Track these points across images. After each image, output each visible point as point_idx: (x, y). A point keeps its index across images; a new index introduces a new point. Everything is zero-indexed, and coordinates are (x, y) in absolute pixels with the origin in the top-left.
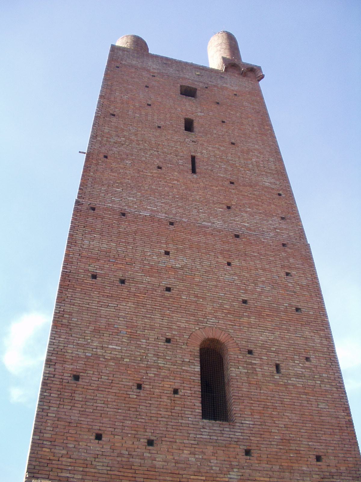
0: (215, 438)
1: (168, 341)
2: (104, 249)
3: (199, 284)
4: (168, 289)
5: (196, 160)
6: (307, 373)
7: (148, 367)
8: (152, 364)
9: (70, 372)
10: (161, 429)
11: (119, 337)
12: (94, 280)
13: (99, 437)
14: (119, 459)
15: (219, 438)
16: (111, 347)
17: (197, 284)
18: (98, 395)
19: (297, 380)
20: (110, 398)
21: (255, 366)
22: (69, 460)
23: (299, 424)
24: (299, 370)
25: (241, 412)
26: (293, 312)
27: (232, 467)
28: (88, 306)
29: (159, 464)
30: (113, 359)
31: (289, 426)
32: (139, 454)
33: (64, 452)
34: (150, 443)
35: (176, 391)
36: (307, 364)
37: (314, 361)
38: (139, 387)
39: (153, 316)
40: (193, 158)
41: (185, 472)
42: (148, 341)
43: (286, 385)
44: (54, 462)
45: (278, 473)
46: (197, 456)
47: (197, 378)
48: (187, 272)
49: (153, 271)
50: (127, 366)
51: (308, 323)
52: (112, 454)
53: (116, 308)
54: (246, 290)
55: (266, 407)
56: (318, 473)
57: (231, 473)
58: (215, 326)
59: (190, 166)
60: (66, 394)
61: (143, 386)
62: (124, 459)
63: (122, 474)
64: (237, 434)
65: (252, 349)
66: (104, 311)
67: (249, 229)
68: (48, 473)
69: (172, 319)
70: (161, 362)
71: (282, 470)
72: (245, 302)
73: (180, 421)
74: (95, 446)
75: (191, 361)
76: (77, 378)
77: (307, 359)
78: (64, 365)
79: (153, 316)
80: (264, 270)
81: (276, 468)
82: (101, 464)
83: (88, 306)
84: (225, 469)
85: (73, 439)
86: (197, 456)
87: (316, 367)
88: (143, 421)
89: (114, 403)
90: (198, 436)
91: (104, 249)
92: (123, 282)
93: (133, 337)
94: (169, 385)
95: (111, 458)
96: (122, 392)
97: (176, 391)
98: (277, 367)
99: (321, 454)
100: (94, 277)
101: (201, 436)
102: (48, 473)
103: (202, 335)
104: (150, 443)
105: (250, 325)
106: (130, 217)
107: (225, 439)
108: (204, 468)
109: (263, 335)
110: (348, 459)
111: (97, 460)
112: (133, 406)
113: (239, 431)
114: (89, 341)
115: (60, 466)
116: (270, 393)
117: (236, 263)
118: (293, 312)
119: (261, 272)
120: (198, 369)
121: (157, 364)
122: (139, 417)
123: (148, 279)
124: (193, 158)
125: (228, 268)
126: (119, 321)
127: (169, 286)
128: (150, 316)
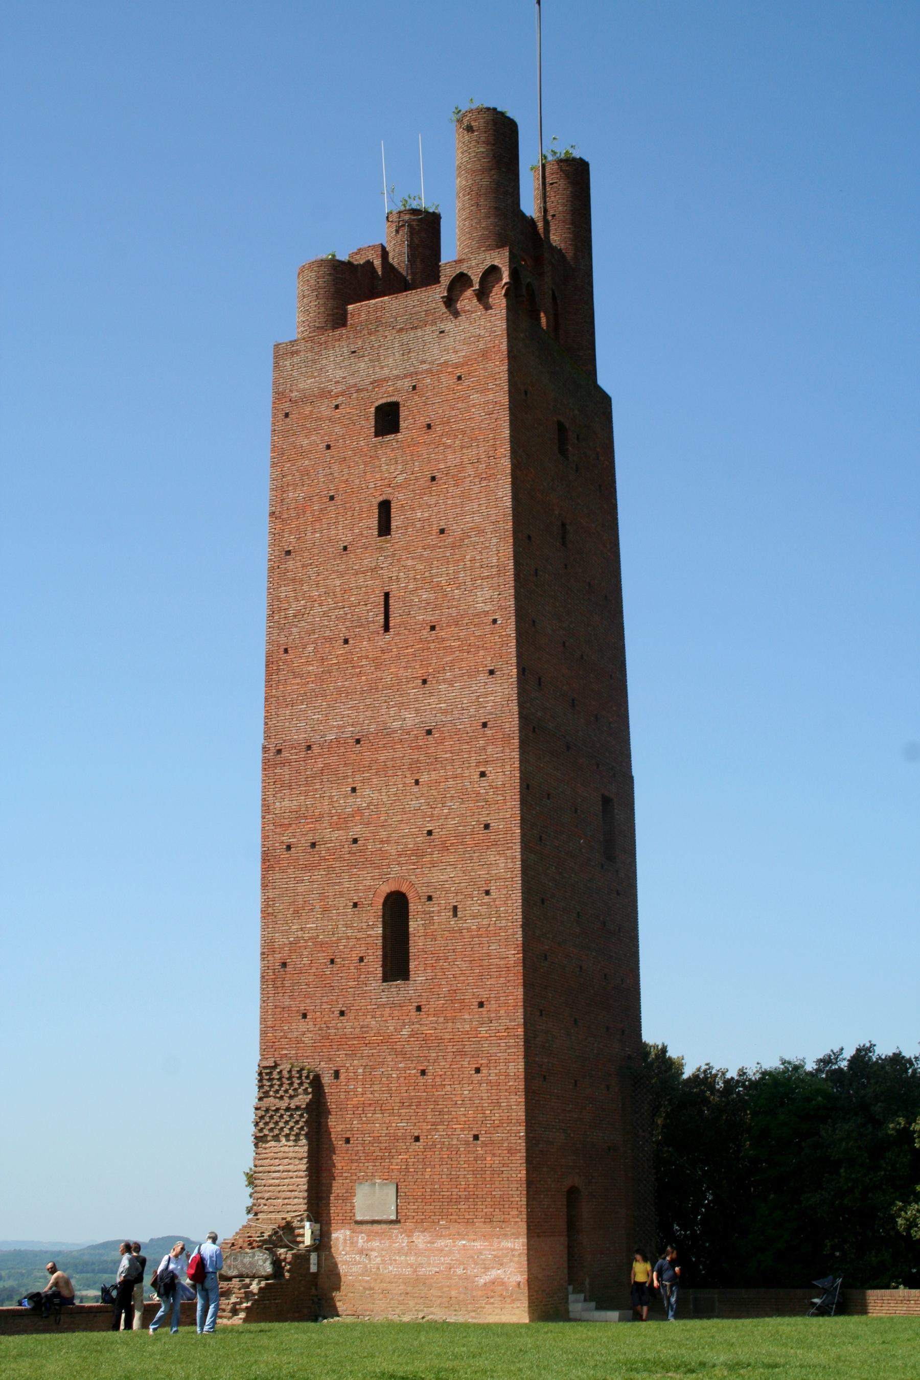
0: (392, 999)
1: (355, 905)
2: (294, 807)
3: (385, 824)
4: (355, 841)
5: (391, 601)
6: (484, 910)
7: (339, 939)
8: (342, 935)
9: (279, 961)
10: (350, 999)
11: (314, 913)
12: (289, 852)
13: (305, 1016)
14: (320, 1032)
15: (396, 999)
16: (308, 926)
17: (382, 824)
18: (302, 978)
19: (472, 921)
20: (311, 978)
21: (432, 915)
22: (286, 1040)
23: (467, 972)
24: (476, 908)
25: (416, 969)
26: (480, 832)
27: (404, 1025)
28: (286, 886)
29: (348, 1031)
30: (310, 938)
31: (458, 976)
32: (334, 1025)
33: (282, 1034)
34: (342, 1013)
35: (361, 959)
36: (486, 899)
37: (494, 894)
38: (332, 961)
39: (341, 881)
40: (387, 595)
41: (368, 1035)
42: (338, 911)
43: (460, 931)
44: (276, 1044)
45: (442, 1025)
46: (377, 1019)
47: (380, 942)
48: (374, 810)
49: (342, 822)
50: (322, 944)
51: (495, 844)
52: (315, 1029)
53: (310, 880)
54: (432, 815)
55: (438, 960)
56: (478, 1019)
57: (403, 1030)
58: (398, 875)
59: (381, 618)
60: (279, 983)
61: (336, 960)
62: (323, 1032)
63: (322, 1044)
64: (410, 992)
65: (431, 894)
66: (301, 888)
67: (445, 712)
68: (273, 1053)
69: (358, 879)
70: (349, 932)
71: (446, 1020)
72: (430, 833)
73: (365, 988)
74: (303, 1026)
75: (375, 923)
76: (284, 965)
77: (487, 893)
78: (275, 955)
79: (341, 881)
80: (455, 777)
81: (441, 1020)
82: (307, 1039)
83: (286, 886)
84: (399, 1027)
85: (287, 1022)
86: (377, 1019)
87: (494, 900)
88: (336, 994)
89: (314, 983)
90: (379, 1000)
91: (294, 807)
92: (313, 845)
93: (325, 910)
94: (355, 956)
95: (314, 1032)
96: (319, 970)
97: (361, 959)
98: (455, 908)
99: (483, 1000)
100: (289, 848)
101: (381, 1000)
102: (273, 1053)
103: (386, 889)
104: (342, 1013)
105: (433, 864)
106: (316, 749)
107: (400, 999)
108: (382, 1029)
109: (444, 874)
110: (509, 1002)
111: (305, 1036)
112: (329, 982)
113: (412, 988)
114: (291, 925)
115: (281, 1047)
116: (443, 942)
117: (424, 779)
118: (480, 832)
119: (451, 782)
120: (380, 931)
121: (345, 935)
122: (333, 991)
123: (337, 834)
124: (387, 595)
125: (416, 789)
126: (313, 896)
127: (355, 837)
128: (338, 881)
